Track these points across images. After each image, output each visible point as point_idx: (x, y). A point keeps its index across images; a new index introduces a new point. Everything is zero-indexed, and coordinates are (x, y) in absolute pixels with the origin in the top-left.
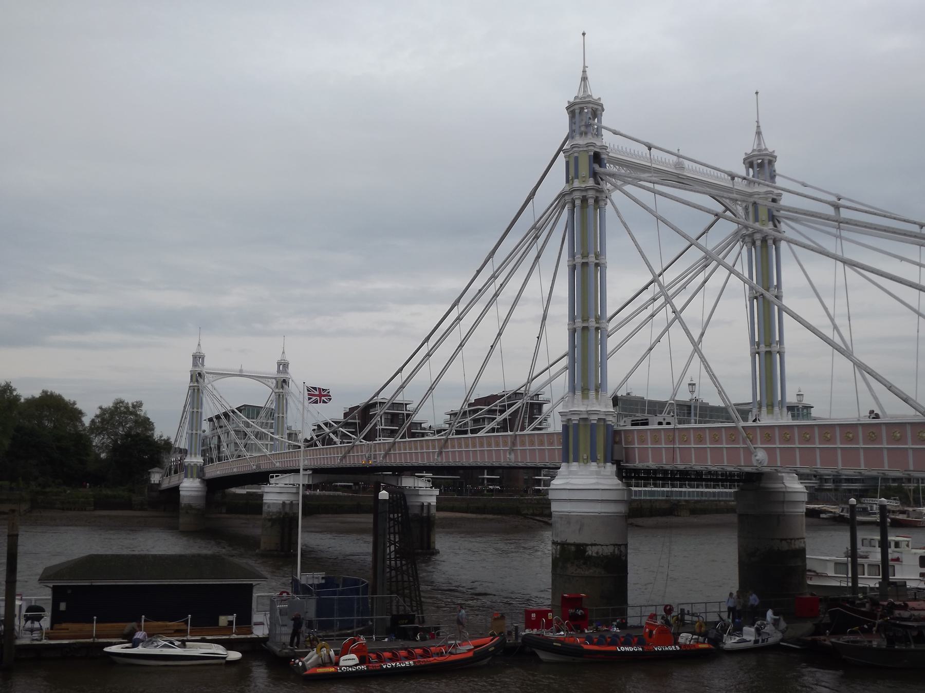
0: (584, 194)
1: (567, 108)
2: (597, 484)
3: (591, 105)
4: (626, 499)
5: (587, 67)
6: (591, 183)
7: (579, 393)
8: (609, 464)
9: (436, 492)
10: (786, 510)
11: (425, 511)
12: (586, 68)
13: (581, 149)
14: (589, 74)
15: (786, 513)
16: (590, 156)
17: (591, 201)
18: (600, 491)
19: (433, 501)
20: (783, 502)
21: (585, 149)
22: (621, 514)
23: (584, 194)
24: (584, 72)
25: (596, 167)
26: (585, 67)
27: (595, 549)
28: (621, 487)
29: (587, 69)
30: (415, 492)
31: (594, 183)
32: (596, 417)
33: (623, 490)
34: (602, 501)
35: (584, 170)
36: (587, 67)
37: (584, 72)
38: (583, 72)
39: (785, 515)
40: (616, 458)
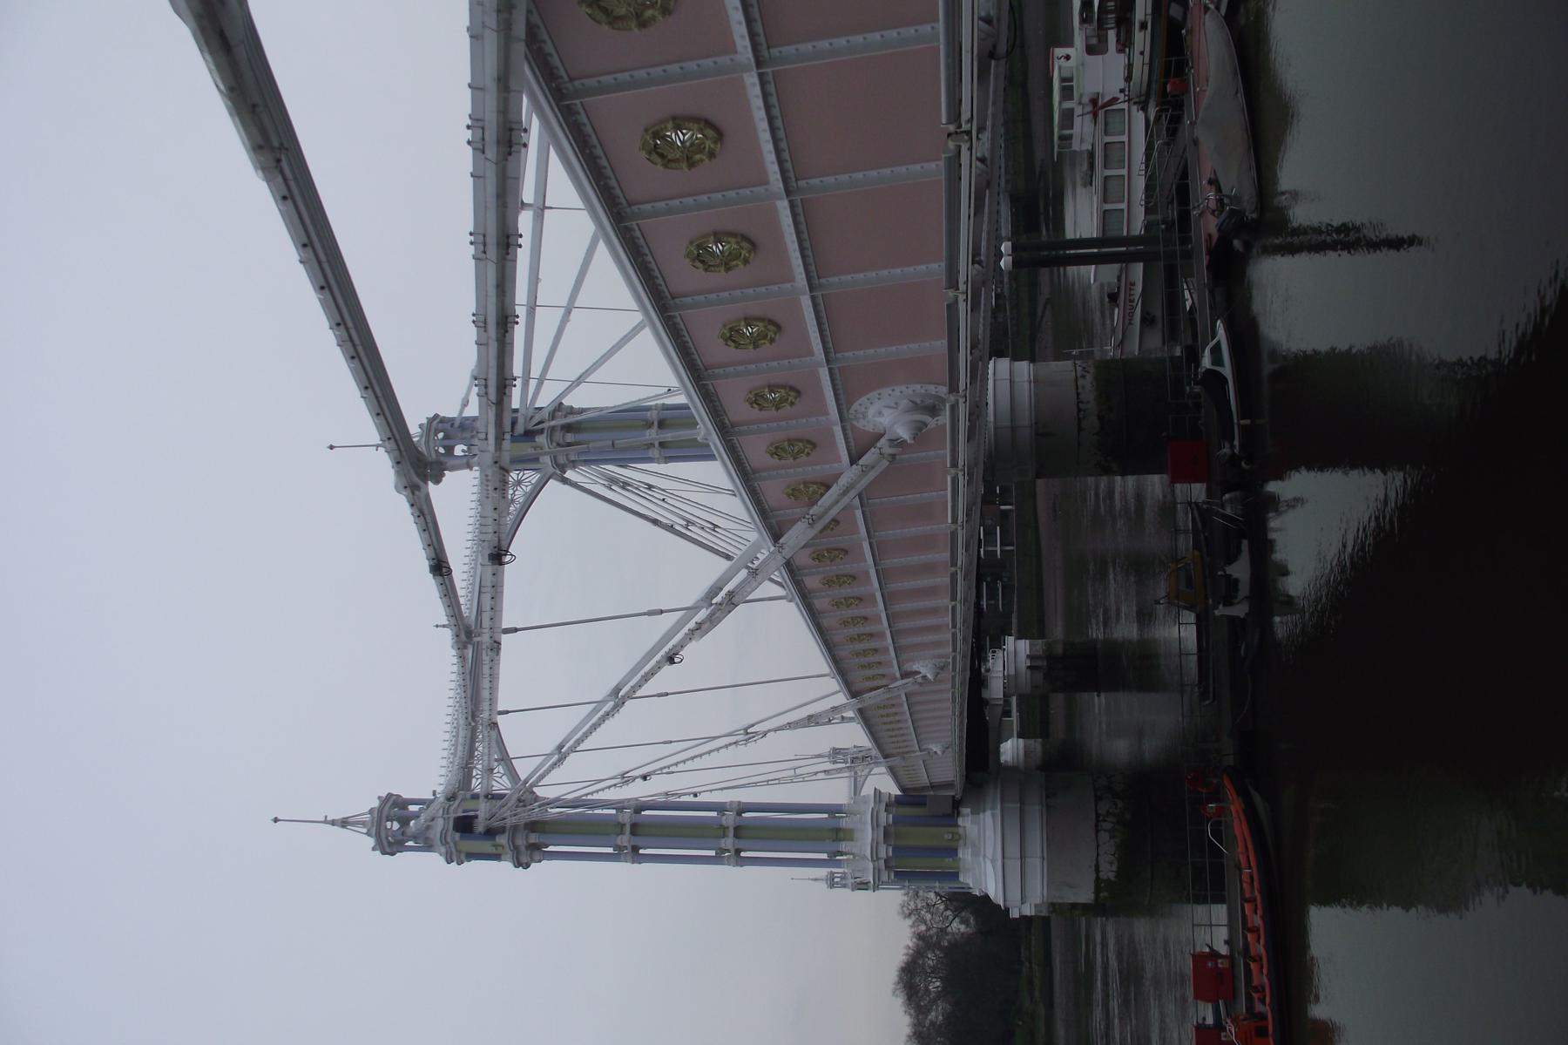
0: (523, 848)
1: (392, 854)
2: (993, 861)
3: (387, 808)
4: (1018, 805)
5: (326, 817)
6: (502, 840)
7: (843, 846)
8: (960, 821)
9: (1010, 640)
10: (1027, 423)
11: (1038, 663)
12: (329, 819)
13: (454, 850)
14: (338, 816)
15: (1033, 422)
16: (461, 837)
17: (534, 838)
18: (1006, 860)
19: (1024, 646)
20: (1014, 428)
21: (452, 845)
22: (1044, 810)
23: (523, 848)
24: (333, 823)
25: (480, 827)
26: (326, 822)
27: (1104, 867)
28: (998, 812)
29: (329, 819)
30: (1010, 682)
31: (503, 836)
32: (883, 815)
33: (1002, 811)
34: (1023, 857)
35: (486, 846)
36: (326, 817)
37: (333, 823)
38: (333, 825)
39: (1036, 423)
40: (949, 811)
